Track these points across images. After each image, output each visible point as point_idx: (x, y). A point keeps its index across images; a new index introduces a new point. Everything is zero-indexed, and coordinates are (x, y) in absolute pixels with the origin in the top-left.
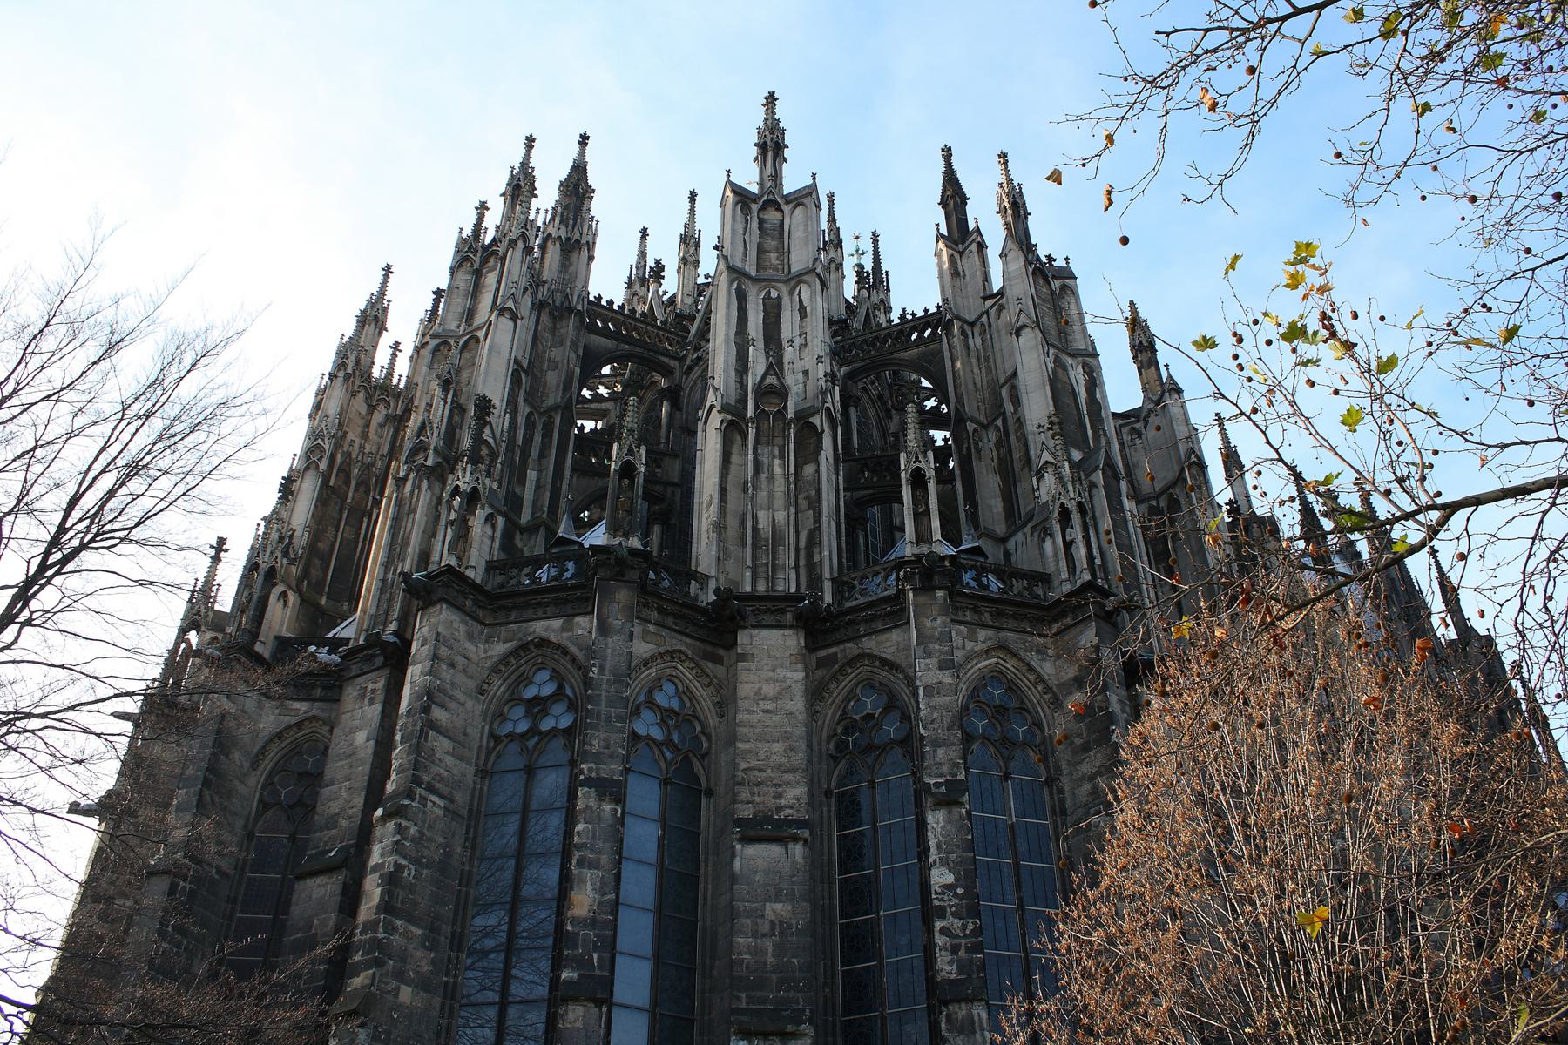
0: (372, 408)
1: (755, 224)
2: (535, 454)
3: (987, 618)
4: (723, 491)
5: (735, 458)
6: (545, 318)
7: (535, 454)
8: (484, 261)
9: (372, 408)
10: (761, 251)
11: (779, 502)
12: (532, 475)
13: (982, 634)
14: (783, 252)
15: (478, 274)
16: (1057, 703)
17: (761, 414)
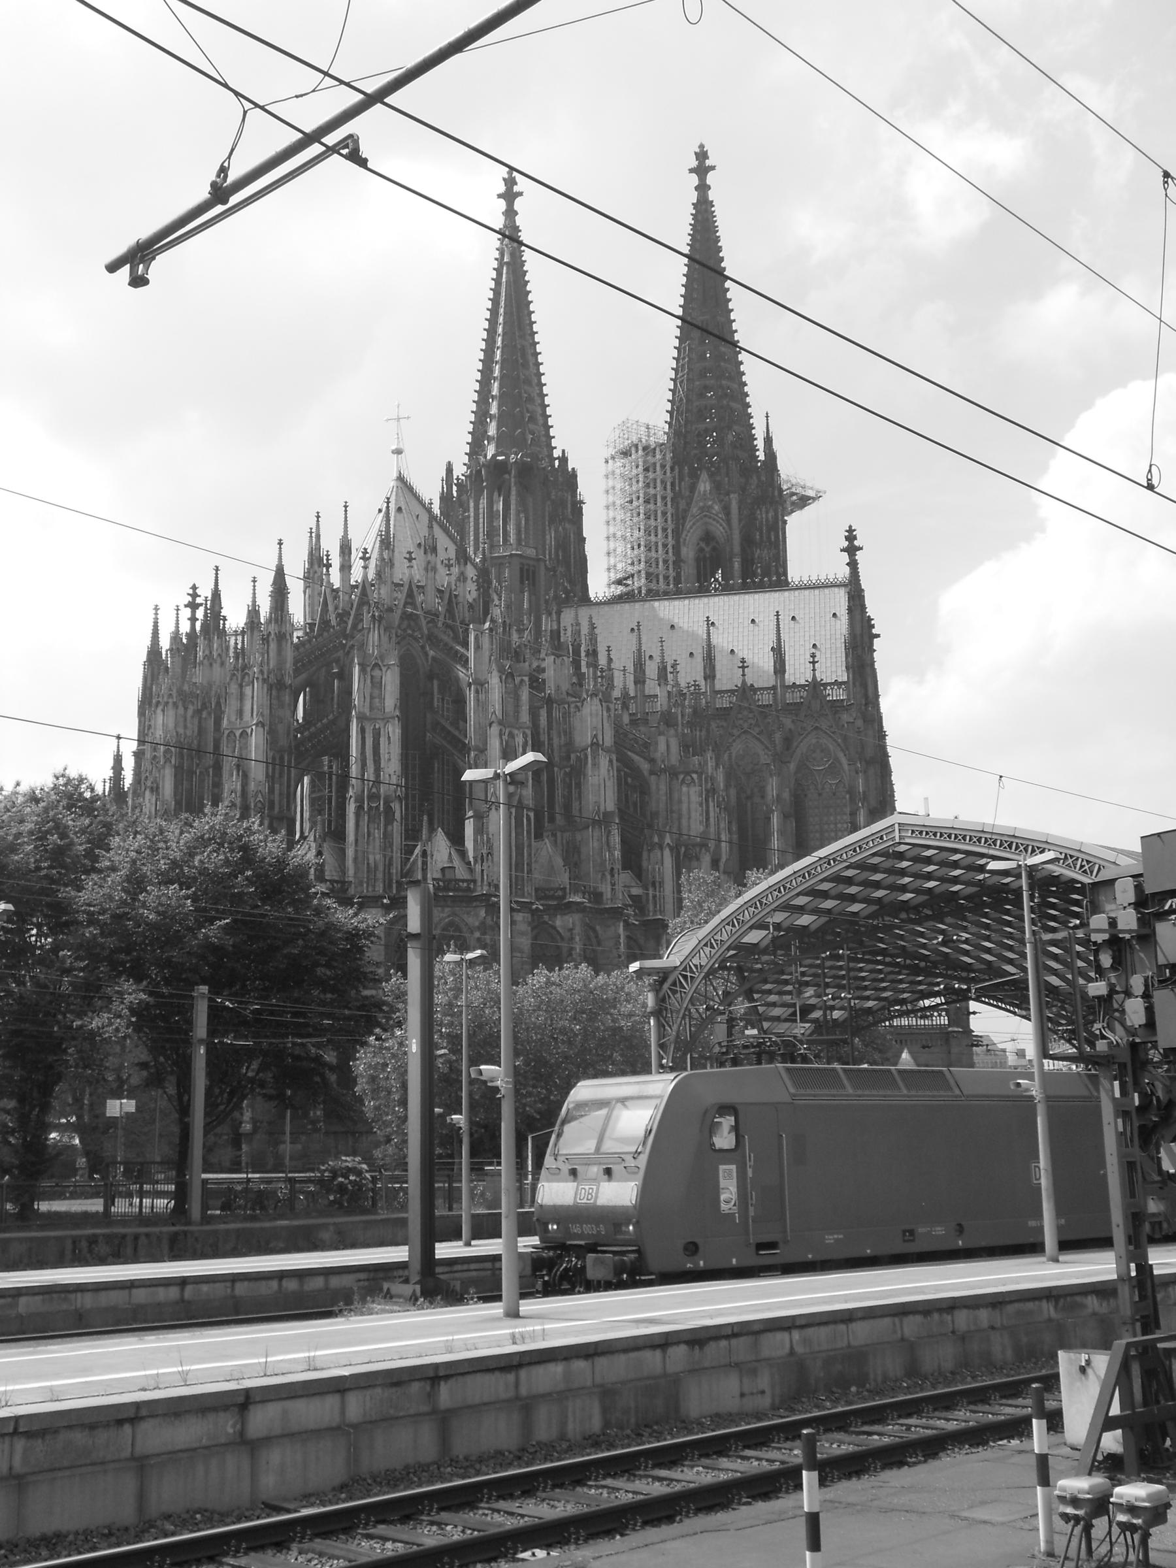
0: (186, 709)
1: (369, 681)
2: (277, 775)
3: (449, 903)
4: (356, 841)
5: (361, 823)
6: (274, 692)
7: (277, 775)
8: (243, 678)
9: (186, 709)
10: (372, 698)
11: (377, 851)
12: (277, 786)
13: (447, 910)
14: (382, 699)
15: (241, 686)
16: (472, 932)
17: (370, 808)
